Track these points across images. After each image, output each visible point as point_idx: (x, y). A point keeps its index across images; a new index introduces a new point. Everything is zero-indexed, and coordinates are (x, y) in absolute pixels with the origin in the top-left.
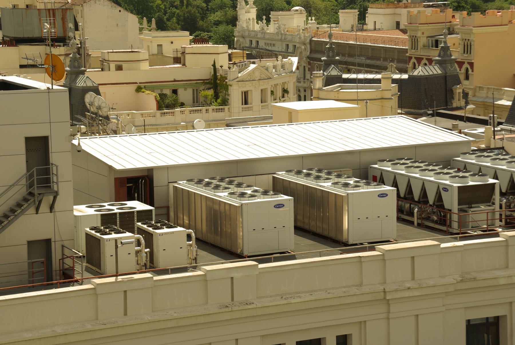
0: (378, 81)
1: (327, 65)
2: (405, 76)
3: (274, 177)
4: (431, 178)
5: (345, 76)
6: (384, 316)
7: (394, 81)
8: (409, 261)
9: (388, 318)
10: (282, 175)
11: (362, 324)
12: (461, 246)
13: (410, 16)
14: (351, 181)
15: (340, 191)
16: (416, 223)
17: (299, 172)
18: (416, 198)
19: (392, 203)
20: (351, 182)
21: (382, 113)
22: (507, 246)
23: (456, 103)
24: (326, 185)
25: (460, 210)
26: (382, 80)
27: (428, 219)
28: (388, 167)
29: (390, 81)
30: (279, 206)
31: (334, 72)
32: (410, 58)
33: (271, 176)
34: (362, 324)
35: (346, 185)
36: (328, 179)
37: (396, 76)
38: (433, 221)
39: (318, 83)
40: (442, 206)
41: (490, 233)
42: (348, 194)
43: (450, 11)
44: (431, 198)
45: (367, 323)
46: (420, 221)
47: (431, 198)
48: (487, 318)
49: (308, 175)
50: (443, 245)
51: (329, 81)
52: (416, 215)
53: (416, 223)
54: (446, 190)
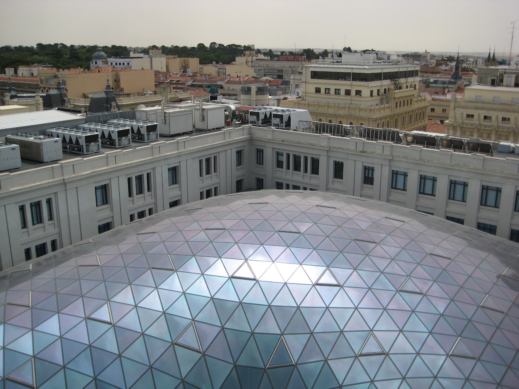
0: (34, 97)
1: (10, 91)
2: (45, 95)
3: (6, 138)
4: (73, 133)
5: (19, 95)
6: (64, 189)
7: (41, 97)
8: (72, 167)
9: (66, 190)
10: (9, 136)
11: (56, 193)
12: (91, 159)
13: (38, 70)
14: (42, 137)
15: (38, 141)
16: (68, 152)
17: (17, 135)
18: (68, 142)
19: (60, 145)
20: (42, 137)
21: (38, 110)
22: (107, 158)
23: (66, 106)
24: (32, 139)
25: (86, 145)
26: (36, 97)
27: (73, 150)
28: (54, 130)
29: (40, 97)
30: (13, 149)
31: (13, 93)
32: (41, 87)
33: (4, 137)
34: (56, 193)
35: (40, 139)
36: (31, 137)
37: (41, 95)
38: (75, 150)
39: (7, 98)
40: (79, 144)
41: (97, 153)
42: (42, 142)
43: (55, 69)
44: (74, 141)
45: (58, 193)
46: (70, 151)
47: (74, 141)
48: (102, 185)
49: (22, 136)
50: (84, 159)
51: (12, 97)
52: (68, 149)
53: (68, 152)
54: (80, 138)
